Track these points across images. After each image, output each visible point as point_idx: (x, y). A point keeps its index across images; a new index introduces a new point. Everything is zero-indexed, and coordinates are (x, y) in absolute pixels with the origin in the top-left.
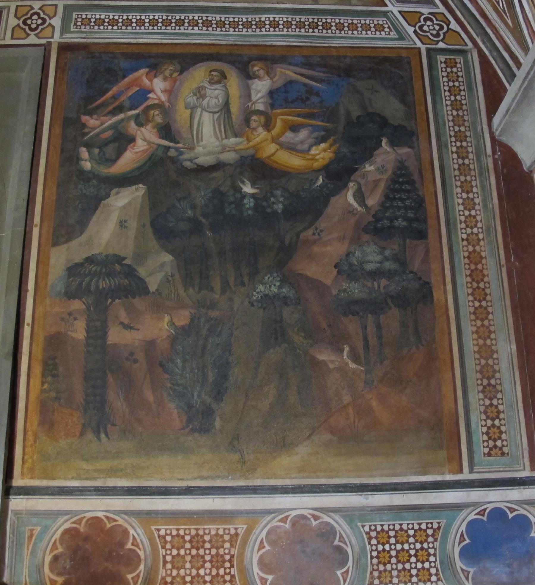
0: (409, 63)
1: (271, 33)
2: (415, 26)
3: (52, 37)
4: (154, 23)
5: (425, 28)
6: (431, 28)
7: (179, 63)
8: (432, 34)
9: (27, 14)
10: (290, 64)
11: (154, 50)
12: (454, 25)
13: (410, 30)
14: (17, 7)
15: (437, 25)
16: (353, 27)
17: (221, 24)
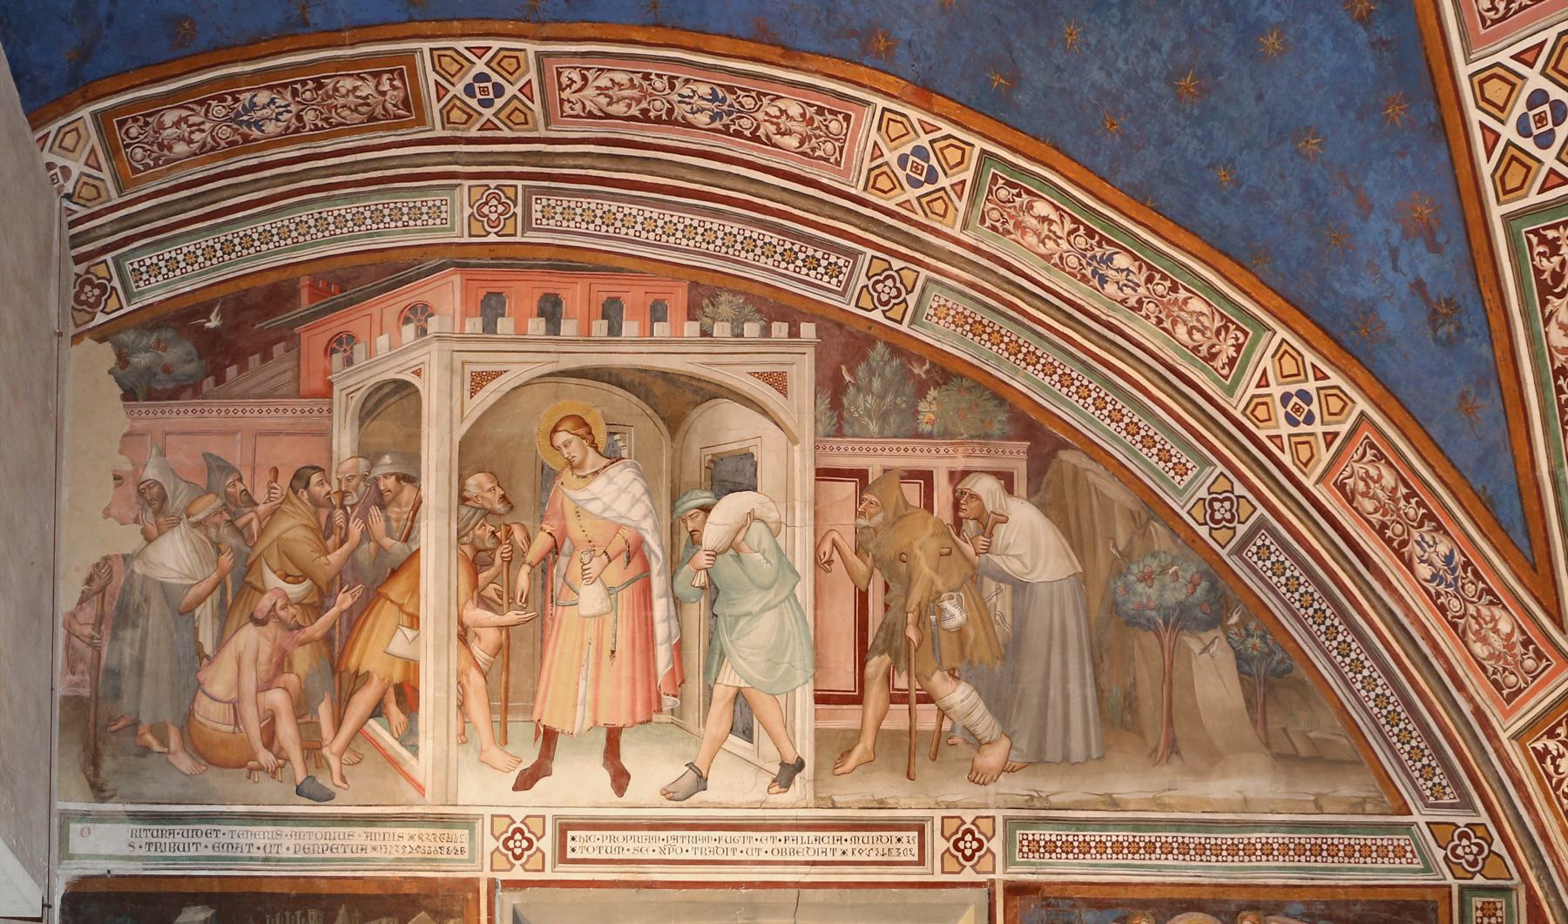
0: (1435, 910)
1: (1263, 864)
2: (1445, 849)
3: (994, 872)
4: (1118, 848)
5: (1460, 851)
6: (1467, 850)
7: (1153, 915)
8: (1467, 861)
9: (956, 832)
10: (1287, 915)
11: (1123, 894)
12: (1498, 846)
13: (1439, 854)
14: (943, 818)
15: (1475, 844)
16: (1365, 851)
17: (1201, 849)
